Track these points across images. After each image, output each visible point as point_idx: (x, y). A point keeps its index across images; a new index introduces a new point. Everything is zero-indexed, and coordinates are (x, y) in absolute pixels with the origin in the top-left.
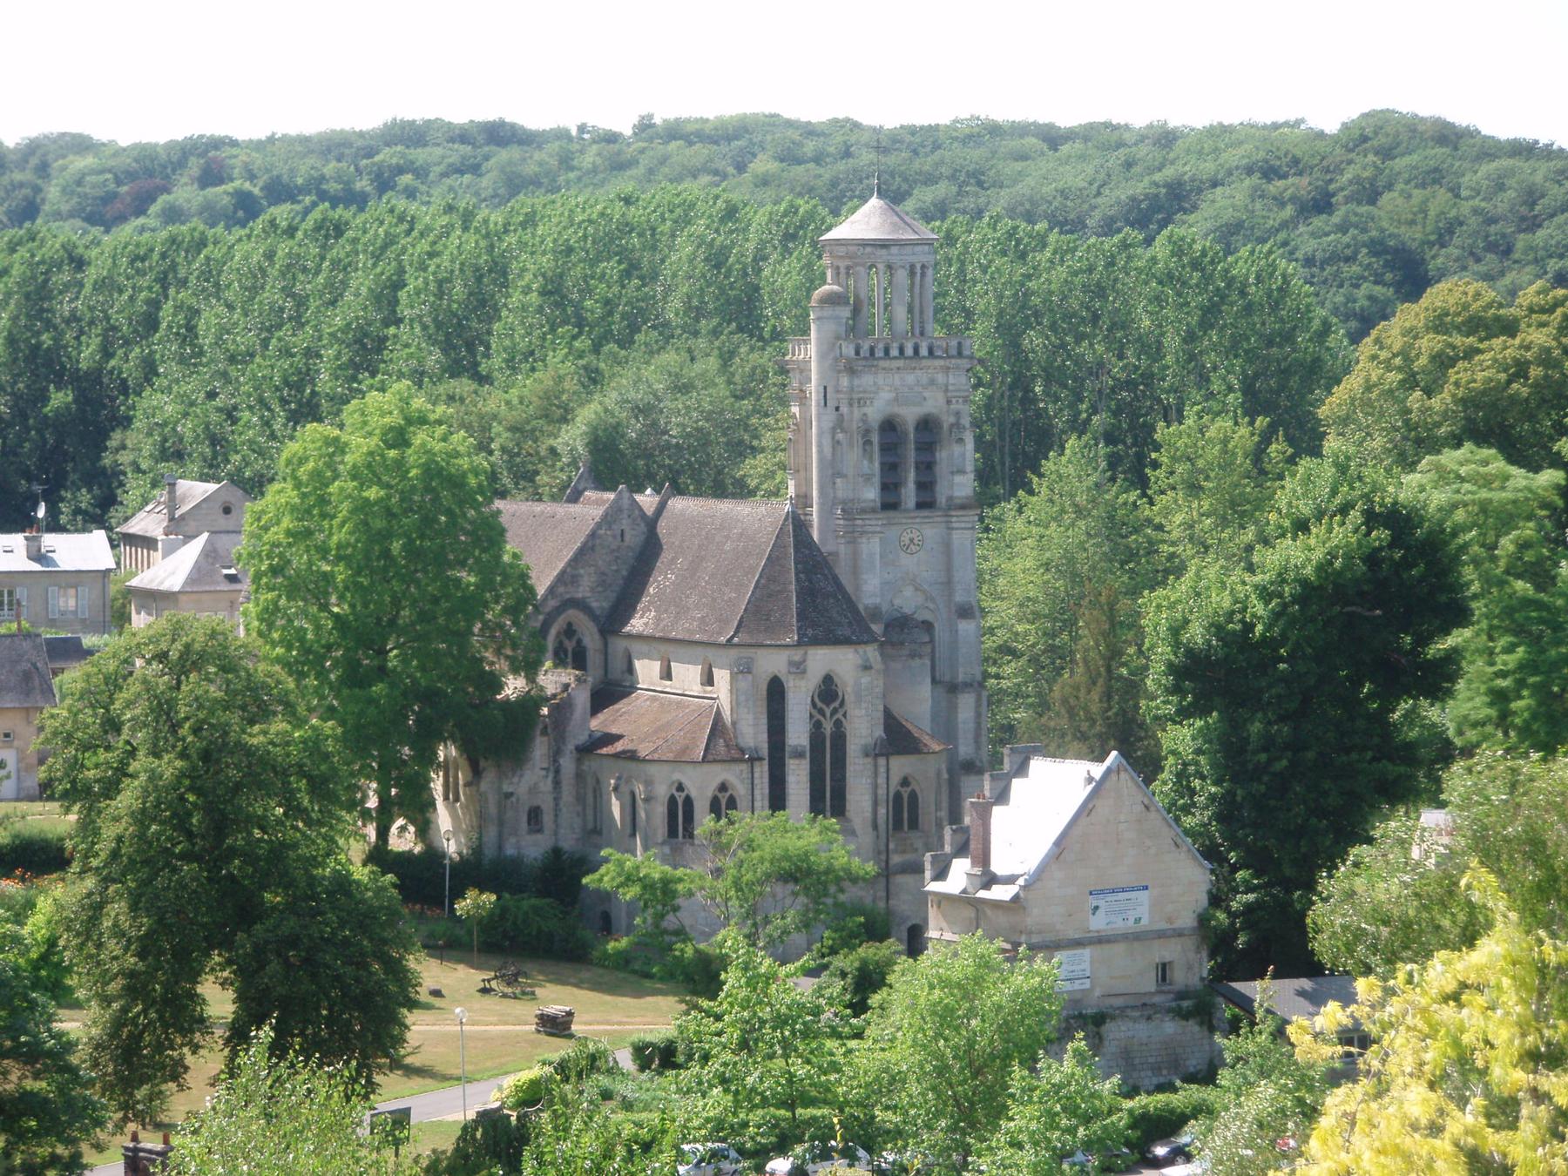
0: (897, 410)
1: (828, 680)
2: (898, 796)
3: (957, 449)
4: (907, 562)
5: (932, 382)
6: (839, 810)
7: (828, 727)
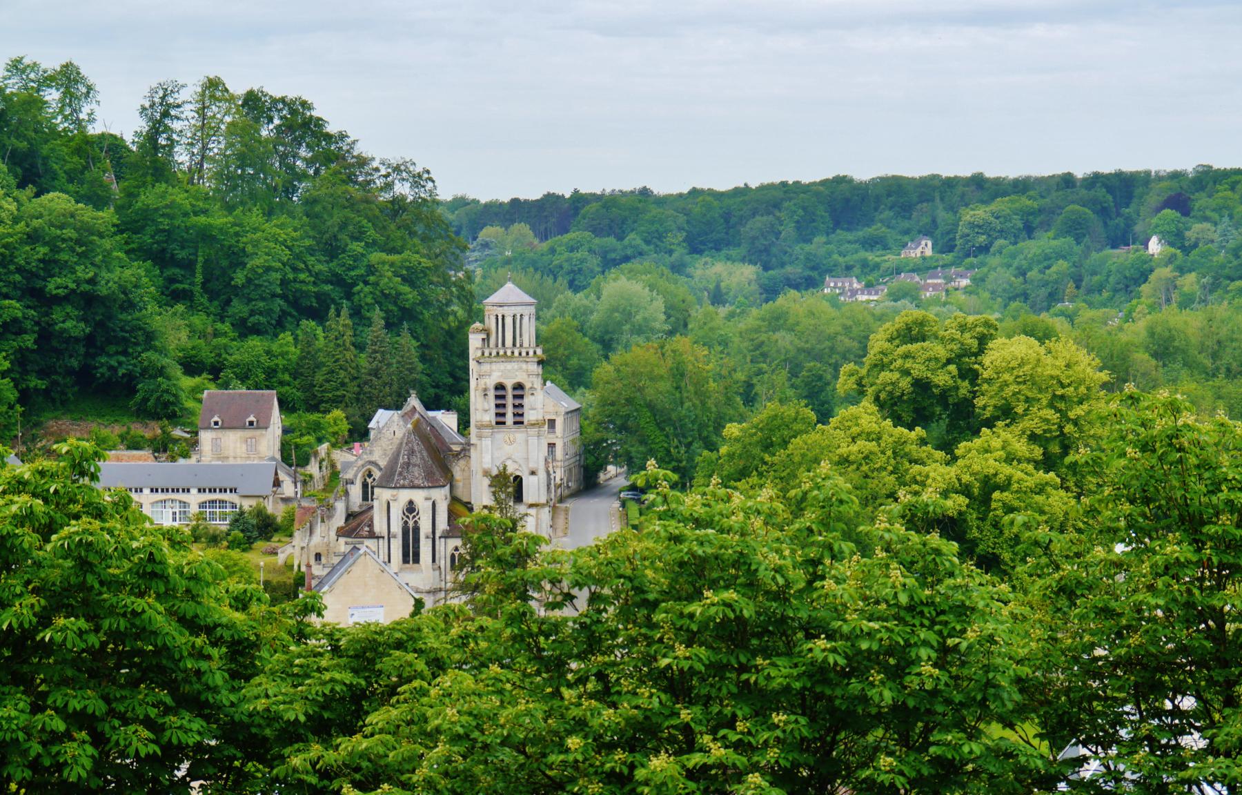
1: (411, 502)
2: (453, 556)
3: (532, 398)
4: (508, 449)
6: (417, 560)
7: (411, 523)
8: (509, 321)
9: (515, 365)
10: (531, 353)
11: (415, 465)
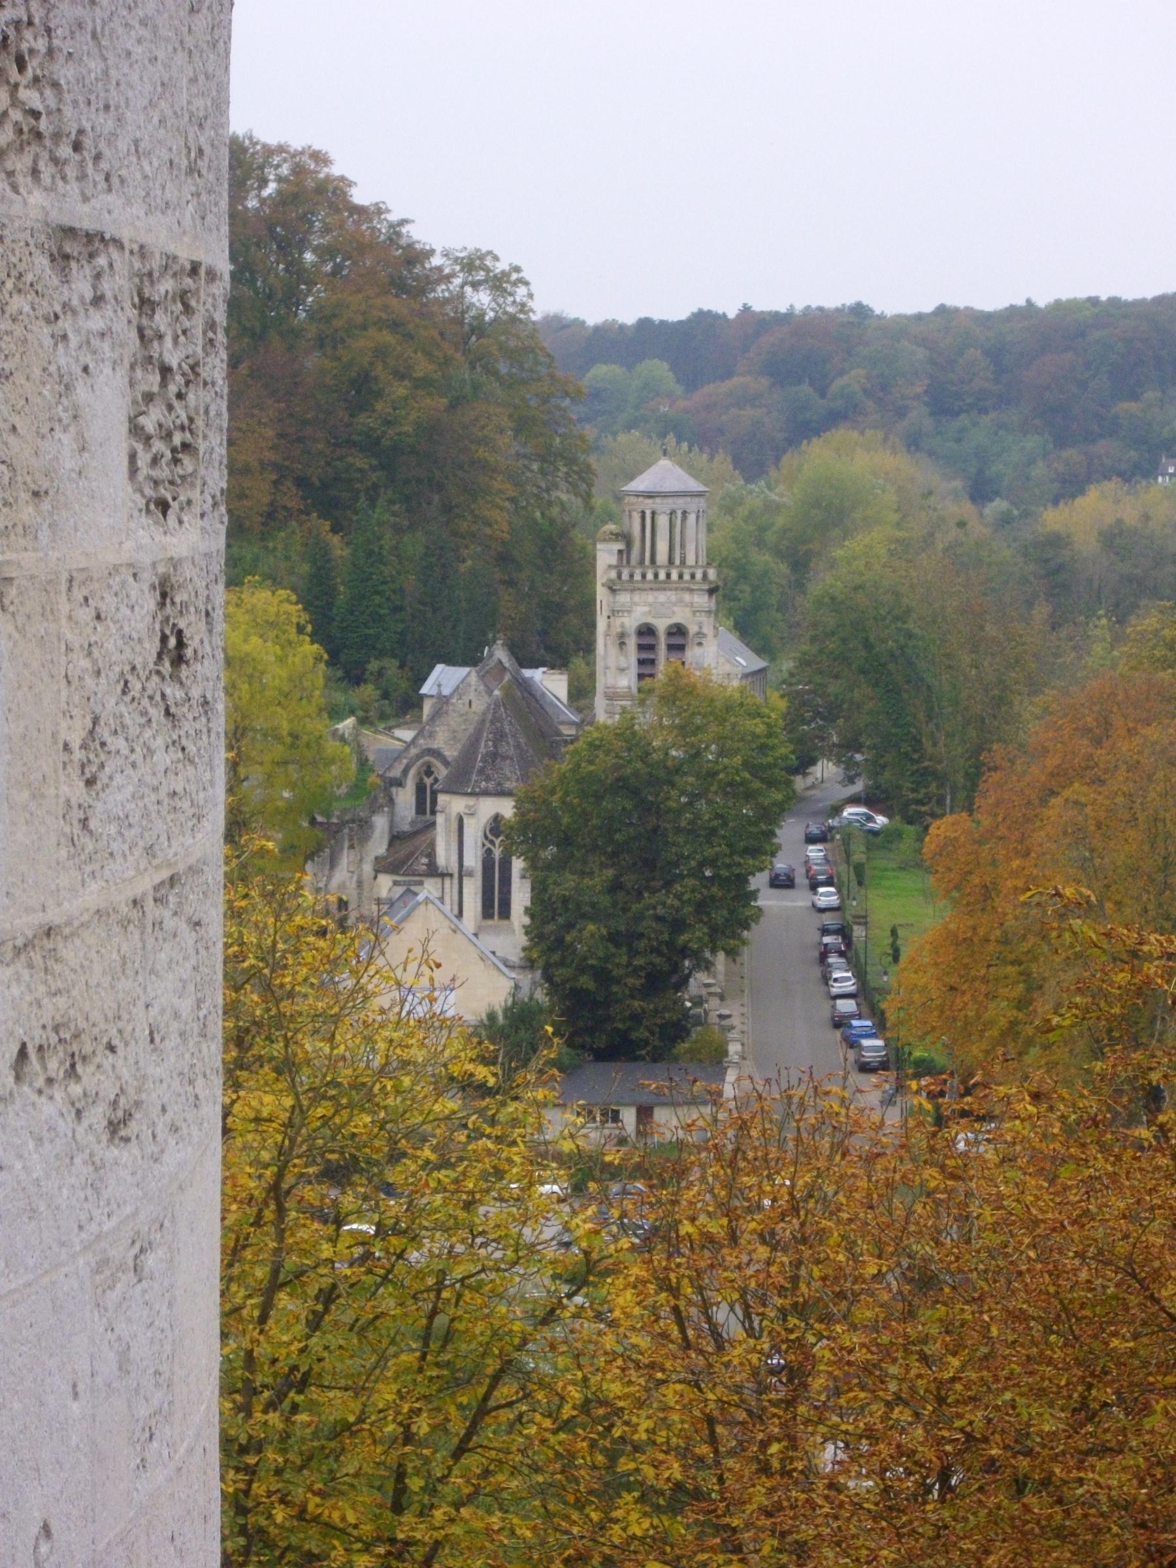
0: (650, 620)
5: (681, 601)
6: (505, 913)
8: (663, 521)
9: (673, 596)
10: (699, 576)
11: (504, 758)
